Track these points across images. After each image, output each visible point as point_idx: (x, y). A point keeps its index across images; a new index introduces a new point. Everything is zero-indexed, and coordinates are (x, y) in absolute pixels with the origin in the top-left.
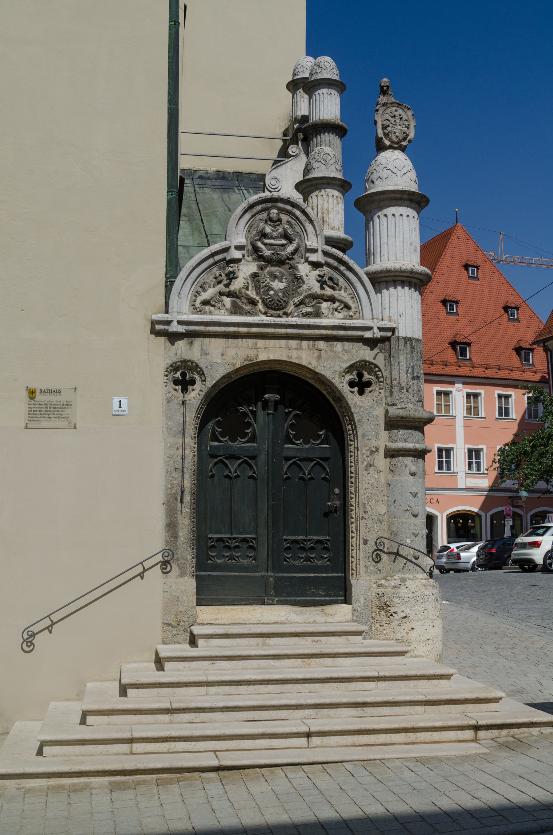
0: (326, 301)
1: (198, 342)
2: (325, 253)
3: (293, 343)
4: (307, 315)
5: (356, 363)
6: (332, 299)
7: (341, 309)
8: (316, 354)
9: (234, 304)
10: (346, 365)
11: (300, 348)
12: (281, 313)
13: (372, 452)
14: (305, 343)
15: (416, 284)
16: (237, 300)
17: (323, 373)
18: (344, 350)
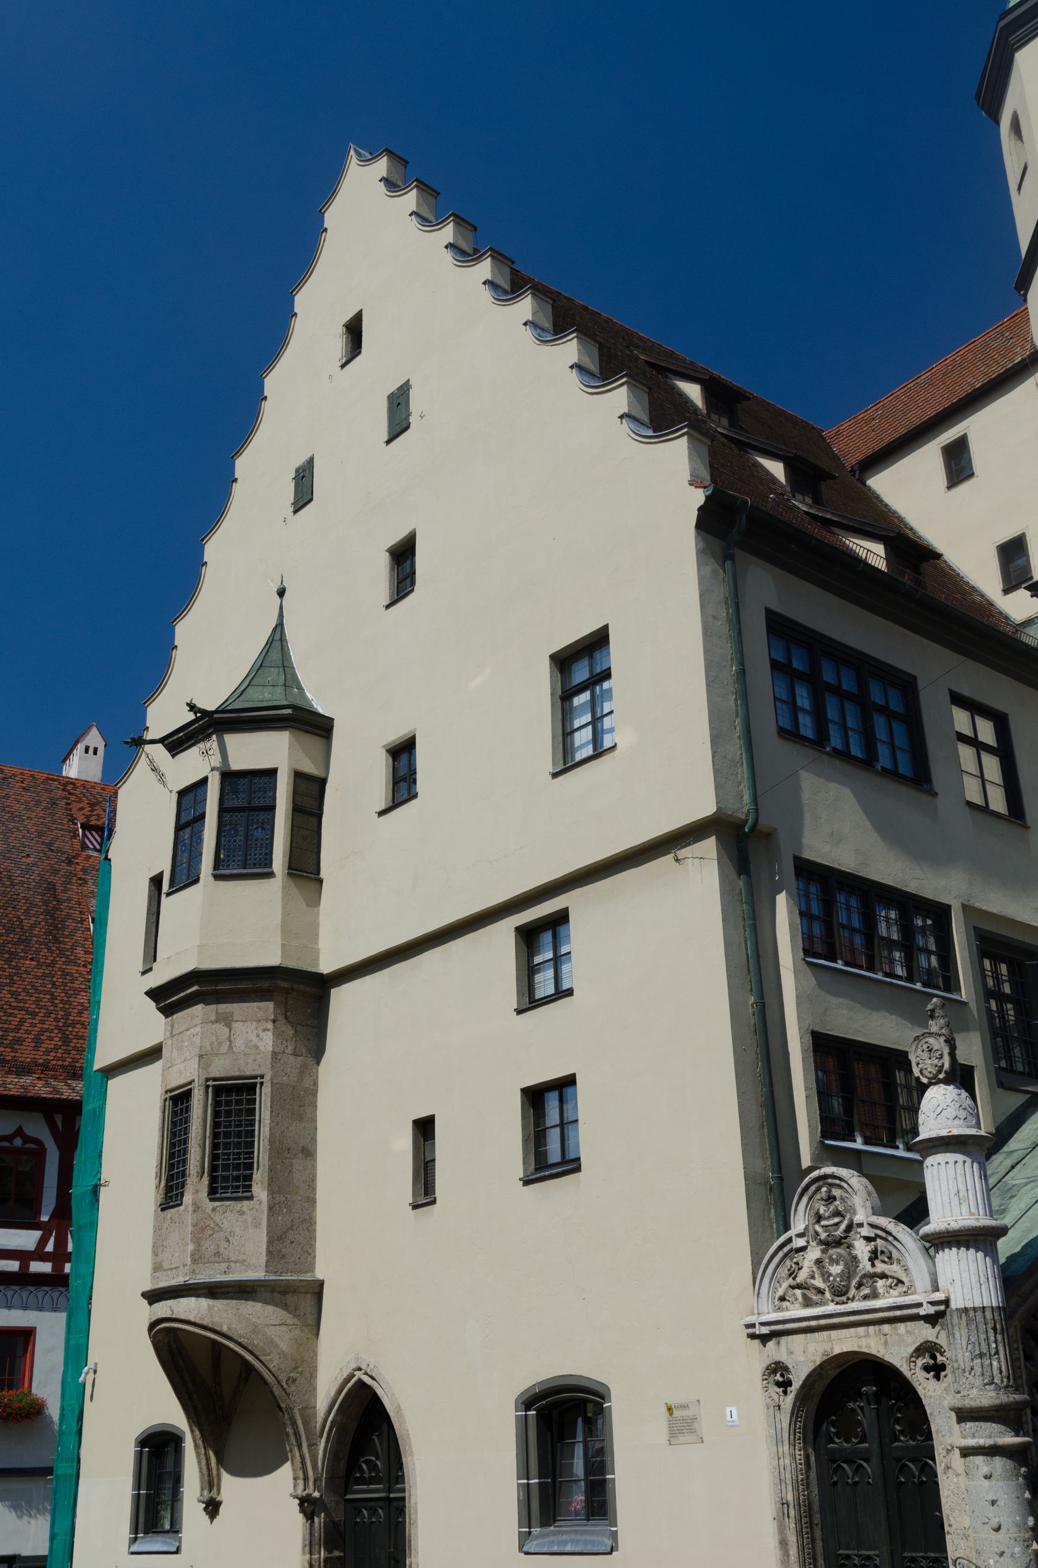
0: (881, 1278)
1: (784, 1340)
2: (872, 1226)
3: (861, 1330)
4: (866, 1297)
5: (921, 1345)
6: (883, 1276)
7: (896, 1285)
8: (883, 1341)
9: (804, 1296)
10: (911, 1349)
11: (867, 1335)
12: (844, 1298)
13: (948, 1451)
14: (871, 1328)
15: (968, 1241)
16: (805, 1291)
17: (891, 1361)
18: (907, 1332)
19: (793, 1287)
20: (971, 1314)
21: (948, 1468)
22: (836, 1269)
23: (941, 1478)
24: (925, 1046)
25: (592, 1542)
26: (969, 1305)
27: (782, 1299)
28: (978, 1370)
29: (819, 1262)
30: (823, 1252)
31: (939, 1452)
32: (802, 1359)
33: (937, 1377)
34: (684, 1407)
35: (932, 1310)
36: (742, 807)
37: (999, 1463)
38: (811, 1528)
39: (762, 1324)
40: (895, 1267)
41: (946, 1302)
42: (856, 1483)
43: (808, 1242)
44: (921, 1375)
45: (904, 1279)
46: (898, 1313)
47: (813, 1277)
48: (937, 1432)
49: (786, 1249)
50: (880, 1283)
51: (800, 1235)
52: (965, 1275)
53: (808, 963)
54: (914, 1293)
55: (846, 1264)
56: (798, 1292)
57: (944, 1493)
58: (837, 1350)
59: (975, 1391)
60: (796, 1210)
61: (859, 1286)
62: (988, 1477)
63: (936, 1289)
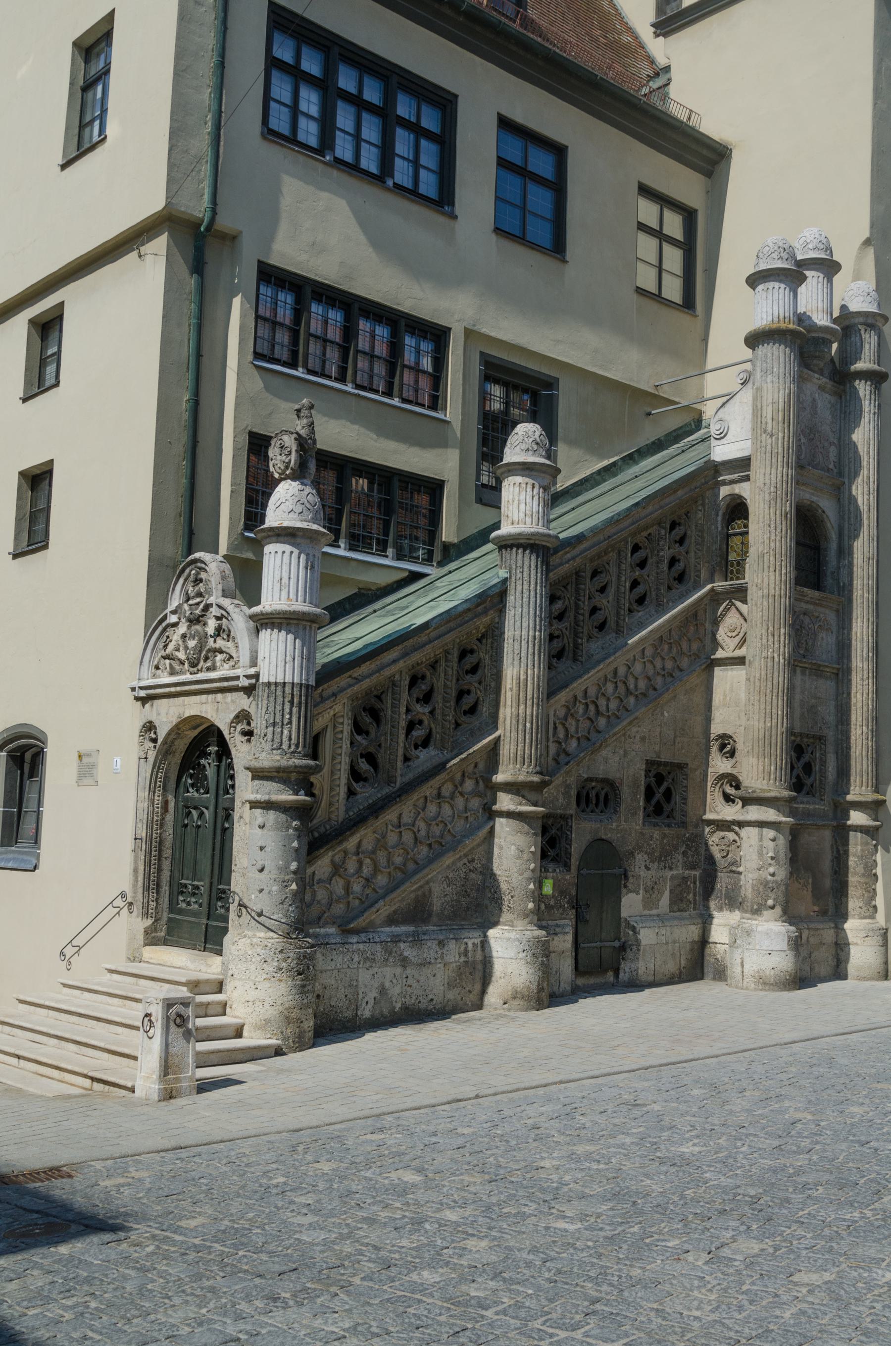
1: (157, 702)
3: (204, 697)
4: (208, 669)
5: (239, 713)
9: (170, 665)
10: (232, 716)
12: (195, 669)
13: (243, 803)
14: (210, 696)
15: (281, 623)
18: (232, 701)
19: (165, 658)
20: (273, 688)
21: (241, 817)
22: (192, 643)
23: (236, 825)
24: (279, 442)
25: (23, 861)
26: (272, 680)
27: (157, 668)
28: (270, 736)
29: (184, 636)
30: (189, 627)
31: (238, 804)
32: (165, 720)
33: (249, 741)
34: (89, 755)
35: (245, 682)
36: (198, 207)
37: (272, 816)
38: (159, 860)
39: (141, 688)
40: (230, 644)
41: (257, 676)
42: (199, 827)
43: (179, 619)
44: (239, 738)
45: (234, 655)
46: (226, 684)
47: (178, 650)
48: (239, 787)
49: (164, 624)
50: (219, 657)
51: (174, 612)
52: (274, 654)
53: (257, 367)
54: (239, 668)
55: (200, 639)
56: (167, 661)
57: (236, 838)
58: (187, 715)
59: (264, 754)
60: (173, 590)
61: (206, 659)
62: (262, 827)
63: (254, 663)
